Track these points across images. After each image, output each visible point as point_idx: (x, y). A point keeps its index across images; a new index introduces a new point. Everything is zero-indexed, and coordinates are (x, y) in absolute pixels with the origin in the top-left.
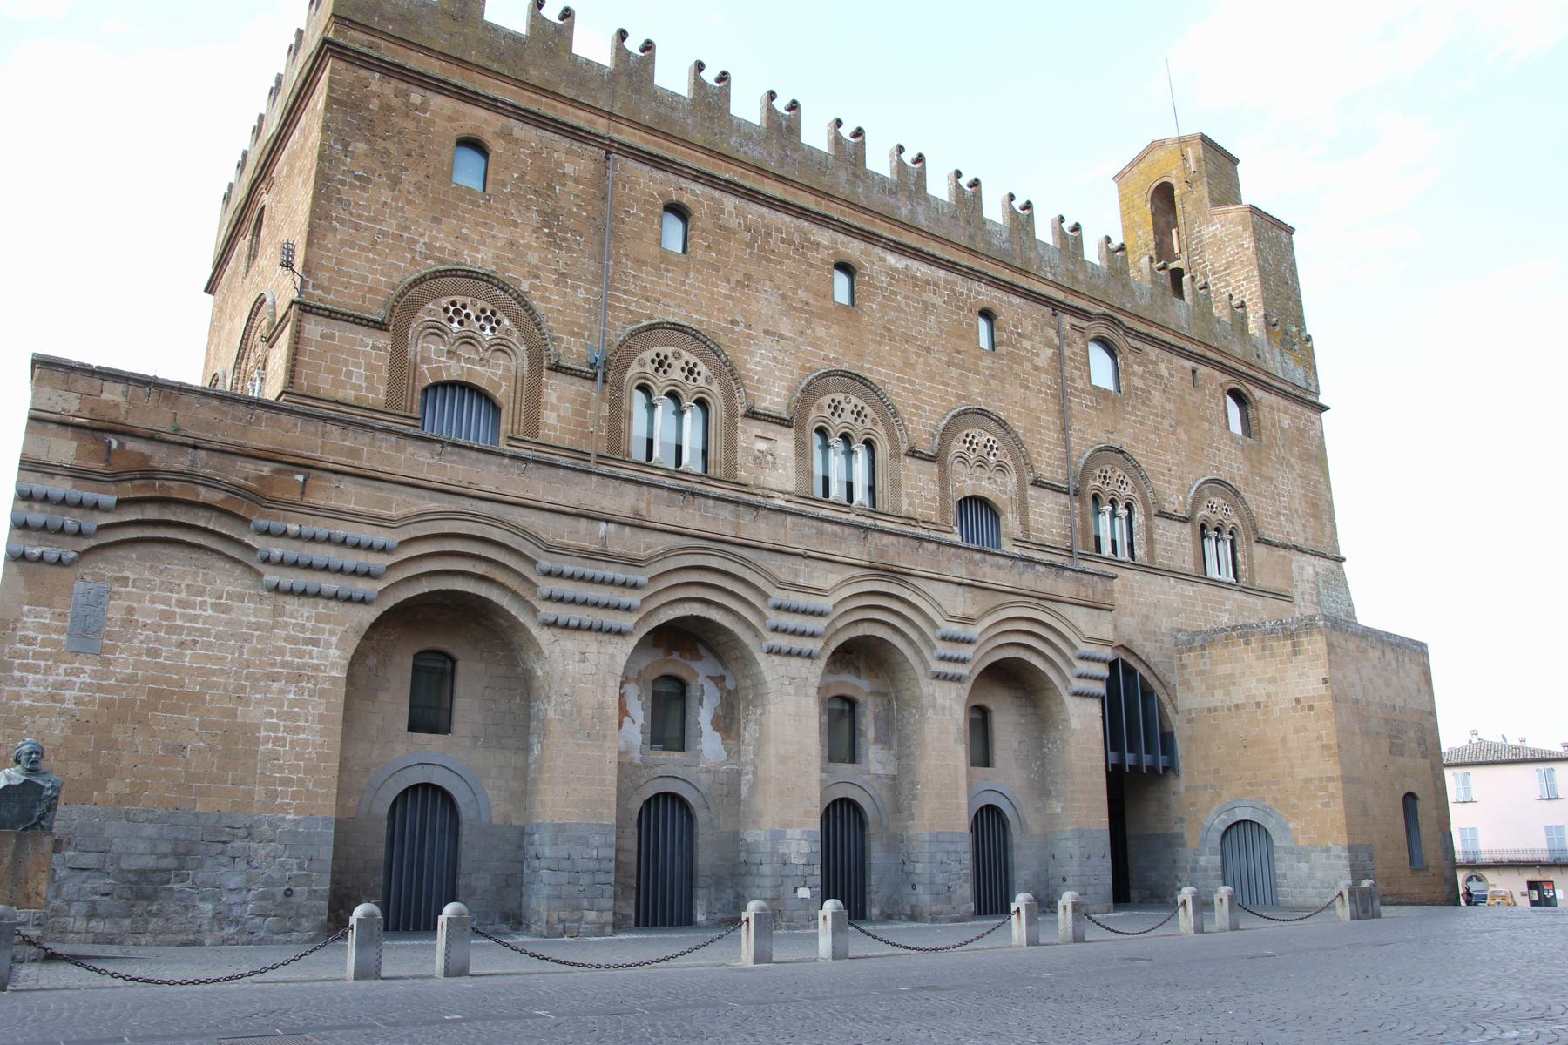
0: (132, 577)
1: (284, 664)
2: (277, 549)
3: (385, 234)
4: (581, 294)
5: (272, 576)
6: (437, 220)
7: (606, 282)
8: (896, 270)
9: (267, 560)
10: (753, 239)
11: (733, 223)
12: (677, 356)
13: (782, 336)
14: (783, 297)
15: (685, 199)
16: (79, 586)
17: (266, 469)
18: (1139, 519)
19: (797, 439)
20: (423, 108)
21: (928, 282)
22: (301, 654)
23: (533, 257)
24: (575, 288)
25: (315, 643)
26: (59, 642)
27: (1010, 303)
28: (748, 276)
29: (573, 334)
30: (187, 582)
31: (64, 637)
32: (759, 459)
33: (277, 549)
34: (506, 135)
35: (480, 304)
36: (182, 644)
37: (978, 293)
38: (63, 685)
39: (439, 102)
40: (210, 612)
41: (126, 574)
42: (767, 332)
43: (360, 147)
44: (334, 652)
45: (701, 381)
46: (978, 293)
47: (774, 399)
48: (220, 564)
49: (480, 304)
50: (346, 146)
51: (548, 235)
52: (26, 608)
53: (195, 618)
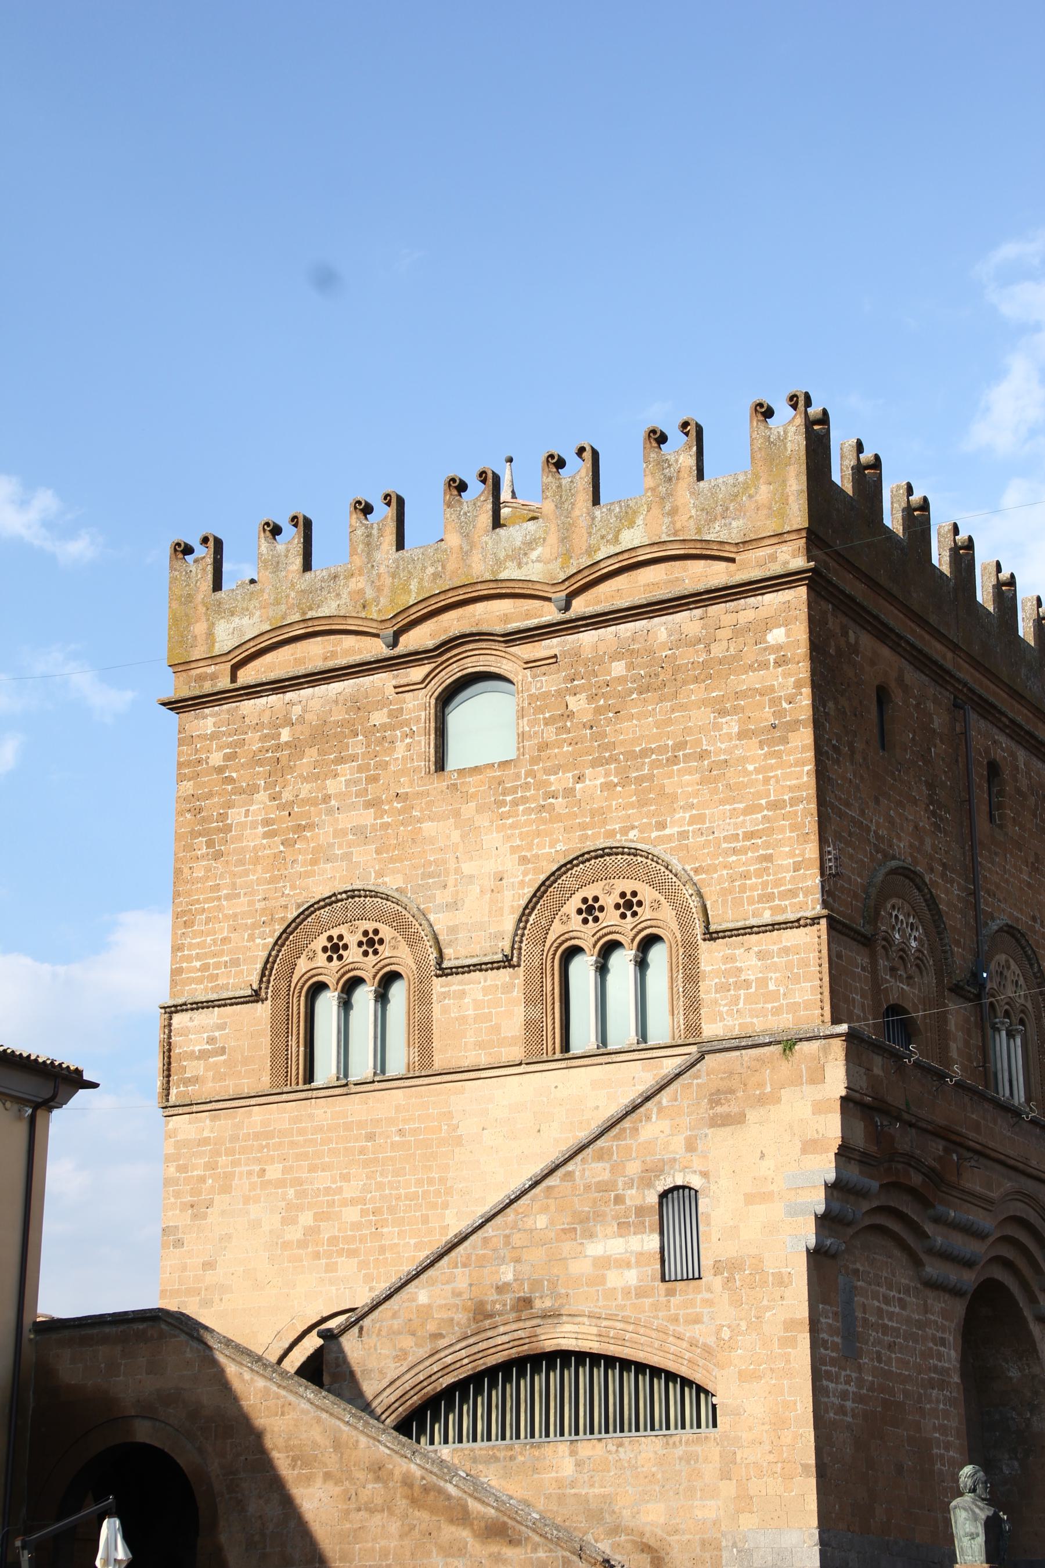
0: (861, 1269)
1: (935, 1369)
2: (939, 1237)
5: (933, 1269)
6: (877, 801)
9: (931, 1251)
11: (1024, 783)
15: (999, 755)
16: (841, 1279)
17: (938, 1147)
20: (855, 649)
22: (940, 1356)
25: (943, 1342)
26: (837, 1344)
30: (885, 1274)
31: (838, 1340)
33: (939, 1237)
34: (900, 680)
35: (906, 906)
36: (891, 1347)
38: (844, 1395)
39: (866, 641)
40: (897, 1310)
41: (858, 1266)
44: (953, 1353)
48: (897, 1253)
51: (934, 813)
52: (821, 1306)
53: (891, 1316)
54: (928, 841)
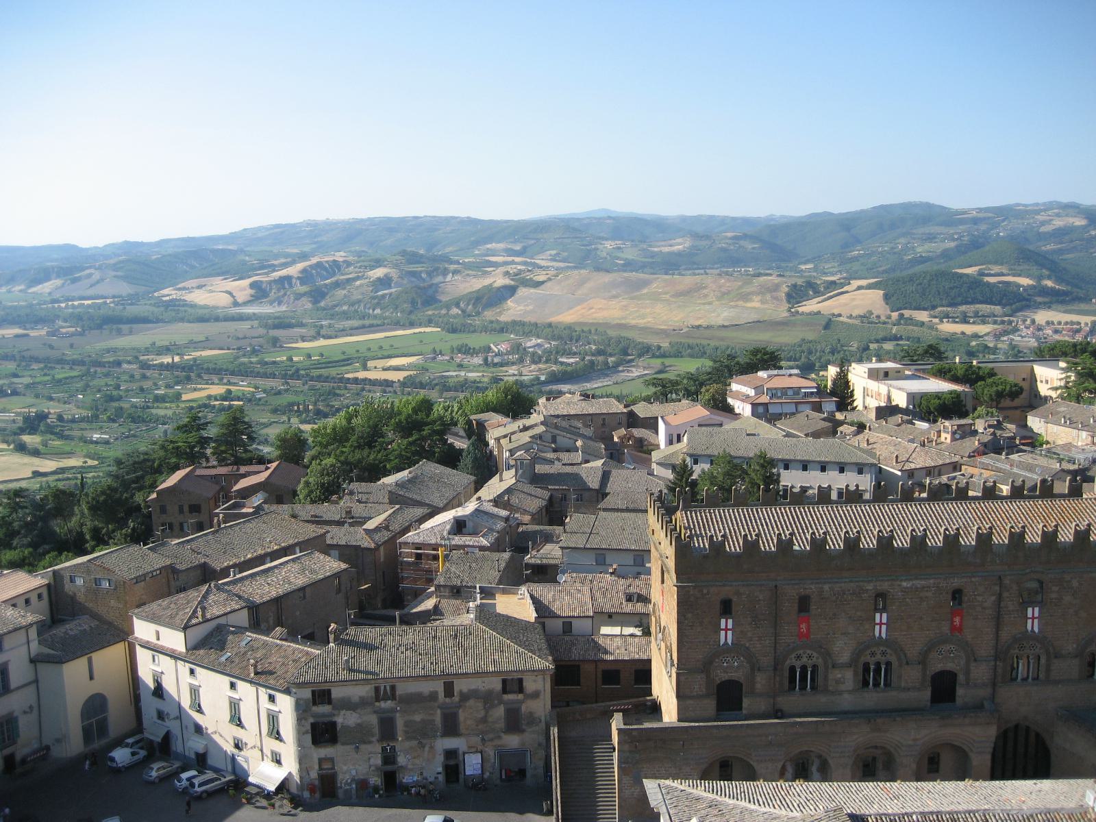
3: (700, 642)
4: (767, 642)
7: (776, 635)
8: (907, 588)
10: (837, 598)
12: (804, 653)
13: (849, 634)
14: (850, 617)
18: (1043, 661)
19: (854, 671)
21: (924, 587)
23: (749, 634)
24: (765, 640)
27: (972, 582)
28: (834, 614)
29: (765, 656)
32: (838, 682)
37: (952, 583)
42: (842, 634)
43: (689, 615)
45: (814, 659)
46: (952, 583)
47: (845, 657)
49: (732, 655)
50: (685, 616)
54: (749, 634)
